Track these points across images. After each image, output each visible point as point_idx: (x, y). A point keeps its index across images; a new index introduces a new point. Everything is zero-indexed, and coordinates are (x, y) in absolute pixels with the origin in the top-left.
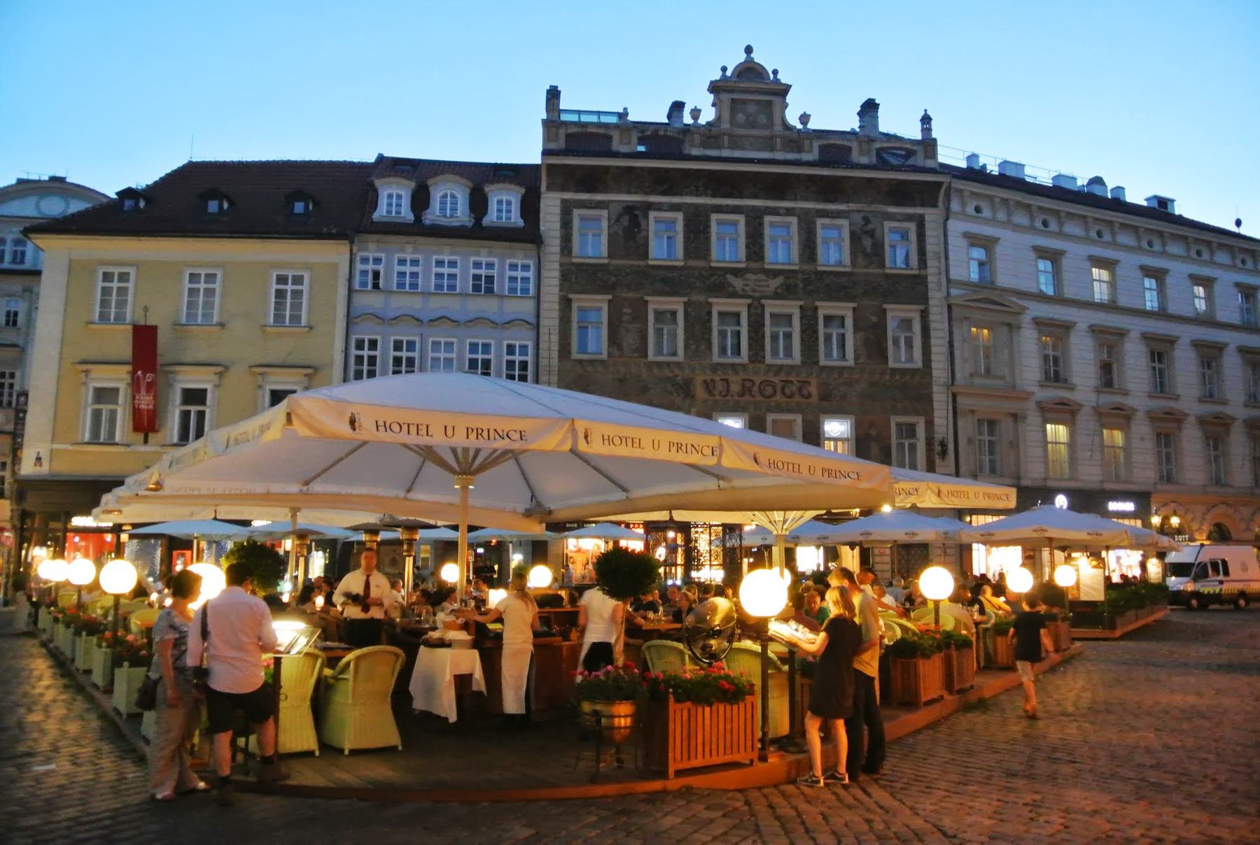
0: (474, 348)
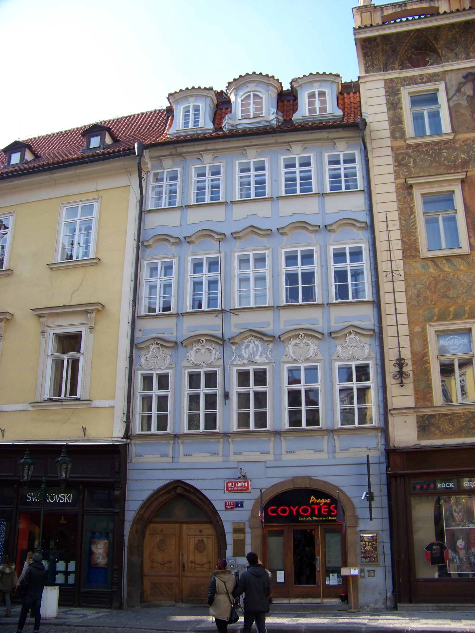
0: (291, 259)
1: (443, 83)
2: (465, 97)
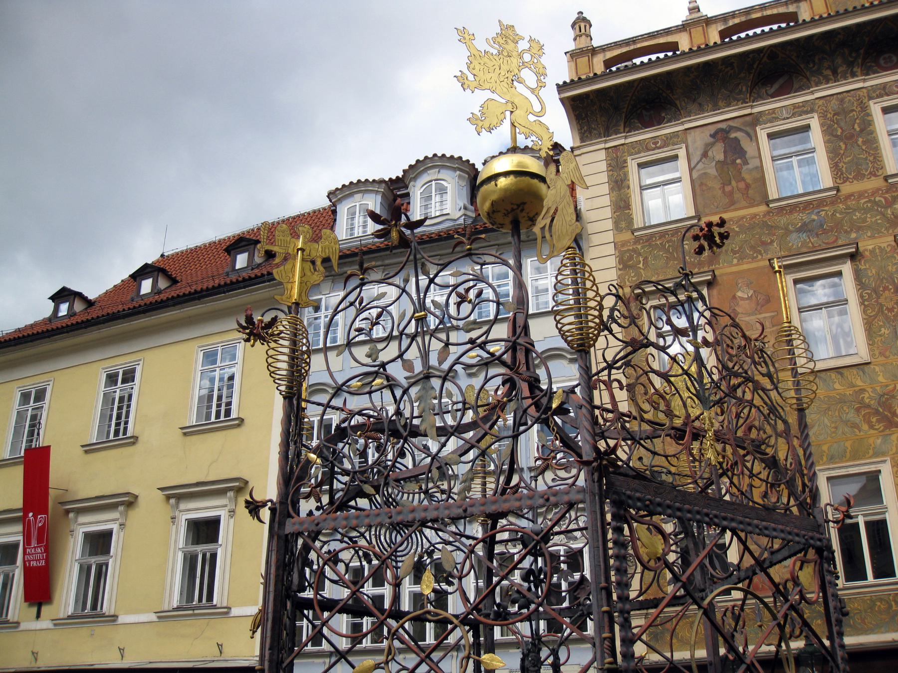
1: (684, 146)
2: (714, 163)
